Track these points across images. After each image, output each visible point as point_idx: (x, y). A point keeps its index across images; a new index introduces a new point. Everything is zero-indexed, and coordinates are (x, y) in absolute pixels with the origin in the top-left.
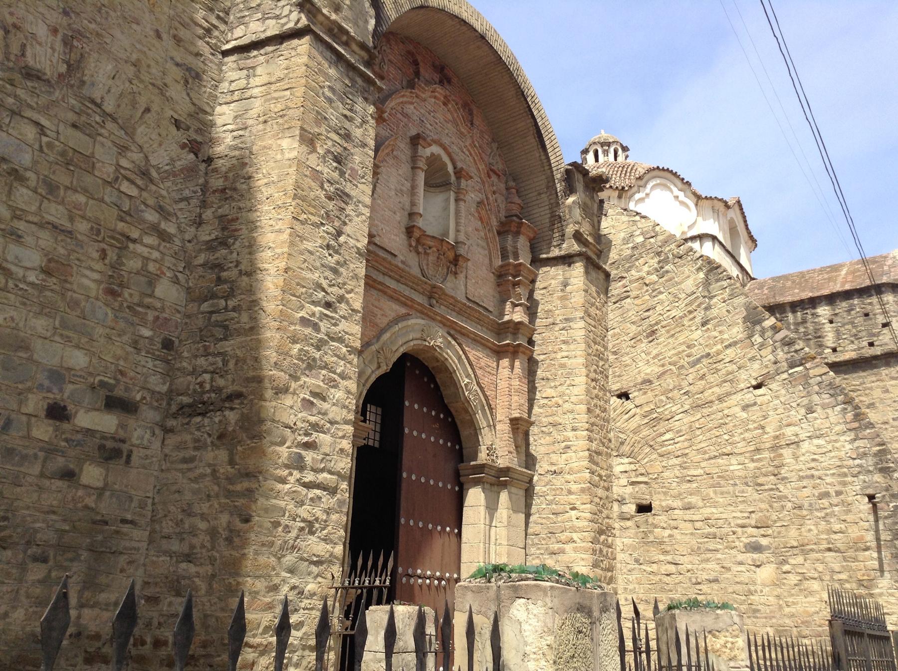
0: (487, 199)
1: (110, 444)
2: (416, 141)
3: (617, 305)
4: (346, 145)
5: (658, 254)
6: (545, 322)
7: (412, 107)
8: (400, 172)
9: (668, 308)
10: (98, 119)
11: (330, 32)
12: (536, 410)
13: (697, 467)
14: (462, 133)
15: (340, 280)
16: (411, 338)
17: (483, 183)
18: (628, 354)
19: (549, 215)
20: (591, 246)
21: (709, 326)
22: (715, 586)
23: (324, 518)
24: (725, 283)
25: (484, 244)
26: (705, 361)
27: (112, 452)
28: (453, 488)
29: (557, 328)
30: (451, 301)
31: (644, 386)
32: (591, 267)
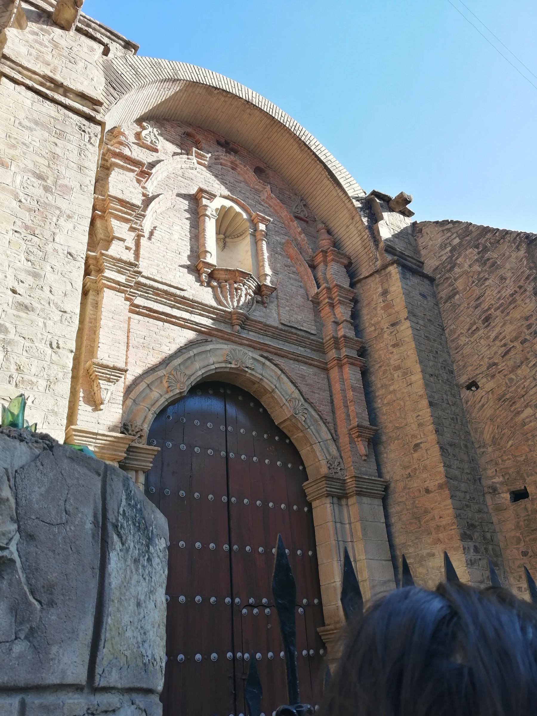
0: (296, 240)
3: (448, 304)
9: (496, 291)
11: (42, 84)
14: (257, 190)
16: (211, 361)
19: (360, 242)
25: (297, 278)
28: (300, 509)
30: (260, 326)
32: (408, 275)
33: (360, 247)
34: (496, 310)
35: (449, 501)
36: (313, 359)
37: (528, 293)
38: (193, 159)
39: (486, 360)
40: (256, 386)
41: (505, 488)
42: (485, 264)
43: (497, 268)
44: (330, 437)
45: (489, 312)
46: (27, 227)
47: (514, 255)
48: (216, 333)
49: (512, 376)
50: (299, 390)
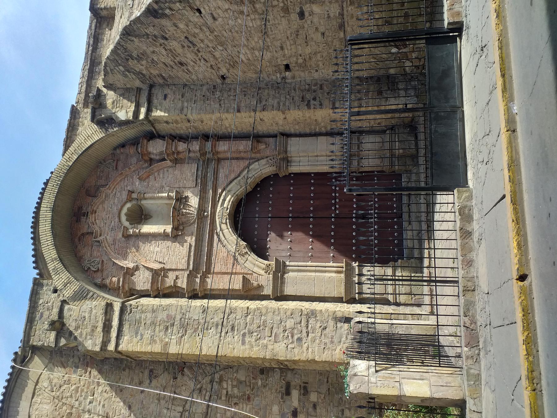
0: (134, 171)
1: (302, 392)
3: (168, 80)
4: (158, 324)
7: (108, 237)
10: (187, 413)
13: (258, 42)
14: (106, 197)
16: (227, 230)
21: (167, 37)
22: (327, 33)
24: (135, 27)
25: (161, 172)
26: (191, 38)
27: (305, 391)
28: (293, 179)
35: (291, 111)
36: (214, 169)
37: (166, 43)
39: (208, 69)
41: (283, 73)
42: (141, 58)
43: (146, 53)
44: (257, 163)
46: (195, 331)
47: (137, 43)
49: (220, 60)
50: (234, 180)
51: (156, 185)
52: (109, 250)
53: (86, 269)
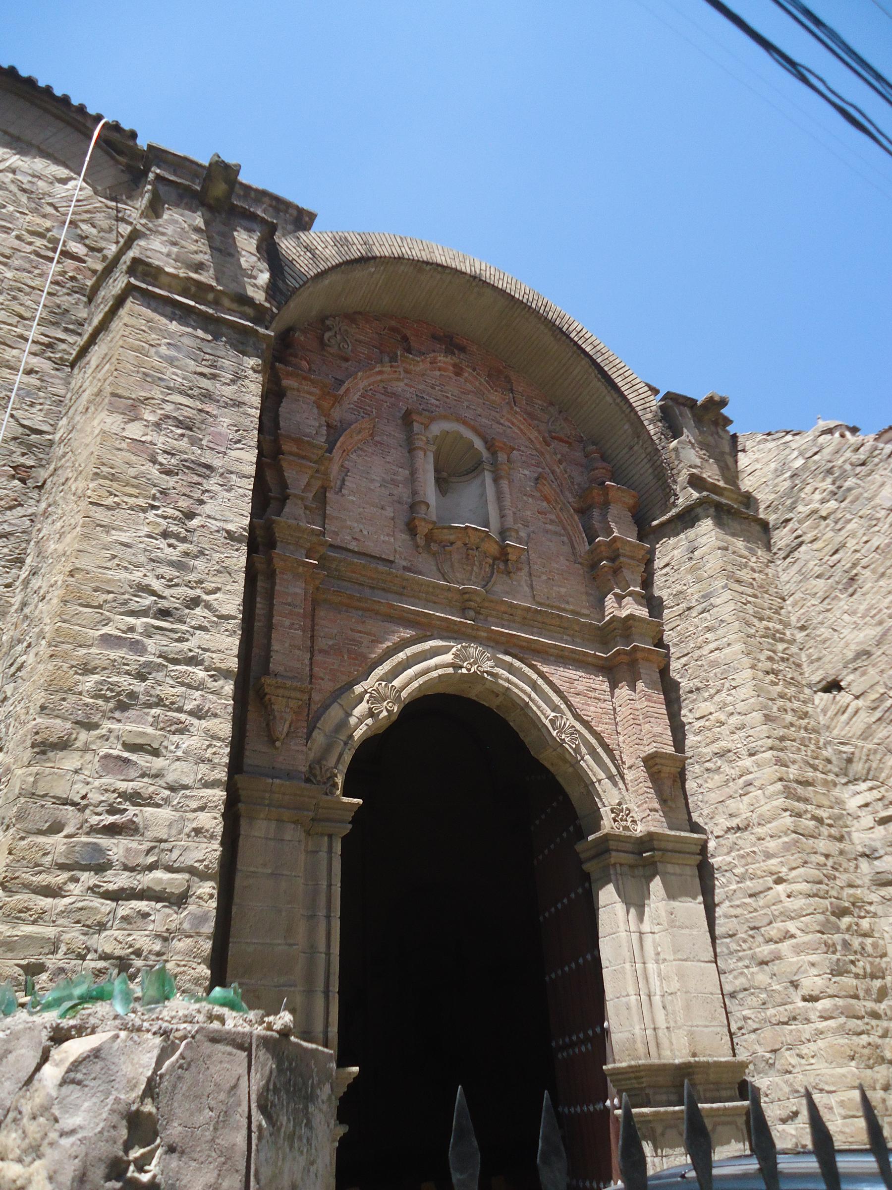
0: (553, 472)
2: (407, 419)
3: (789, 560)
5: (830, 472)
6: (678, 610)
7: (402, 384)
8: (388, 459)
9: (865, 539)
12: (691, 739)
15: (192, 577)
17: (542, 454)
18: (822, 623)
19: (650, 471)
20: (726, 493)
23: (157, 947)
25: (559, 529)
29: (694, 613)
31: (859, 663)
33: (651, 477)
34: (864, 568)
38: (398, 367)
40: (500, 699)
45: (855, 571)
48: (438, 623)
51: (529, 513)
52: (372, 380)
53: (328, 322)
